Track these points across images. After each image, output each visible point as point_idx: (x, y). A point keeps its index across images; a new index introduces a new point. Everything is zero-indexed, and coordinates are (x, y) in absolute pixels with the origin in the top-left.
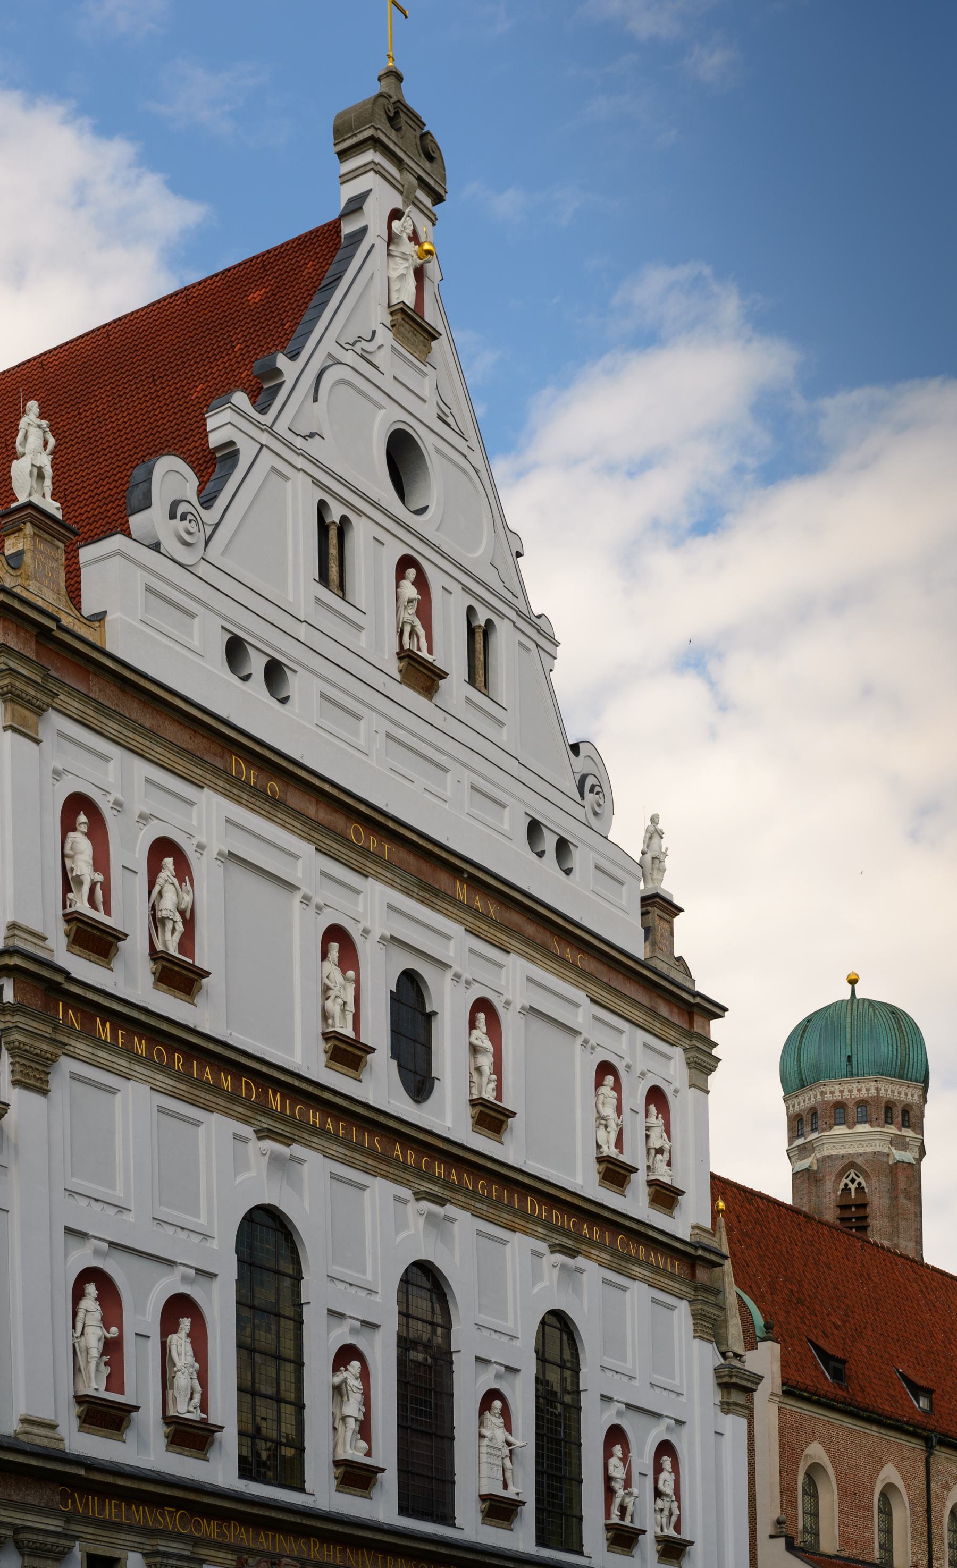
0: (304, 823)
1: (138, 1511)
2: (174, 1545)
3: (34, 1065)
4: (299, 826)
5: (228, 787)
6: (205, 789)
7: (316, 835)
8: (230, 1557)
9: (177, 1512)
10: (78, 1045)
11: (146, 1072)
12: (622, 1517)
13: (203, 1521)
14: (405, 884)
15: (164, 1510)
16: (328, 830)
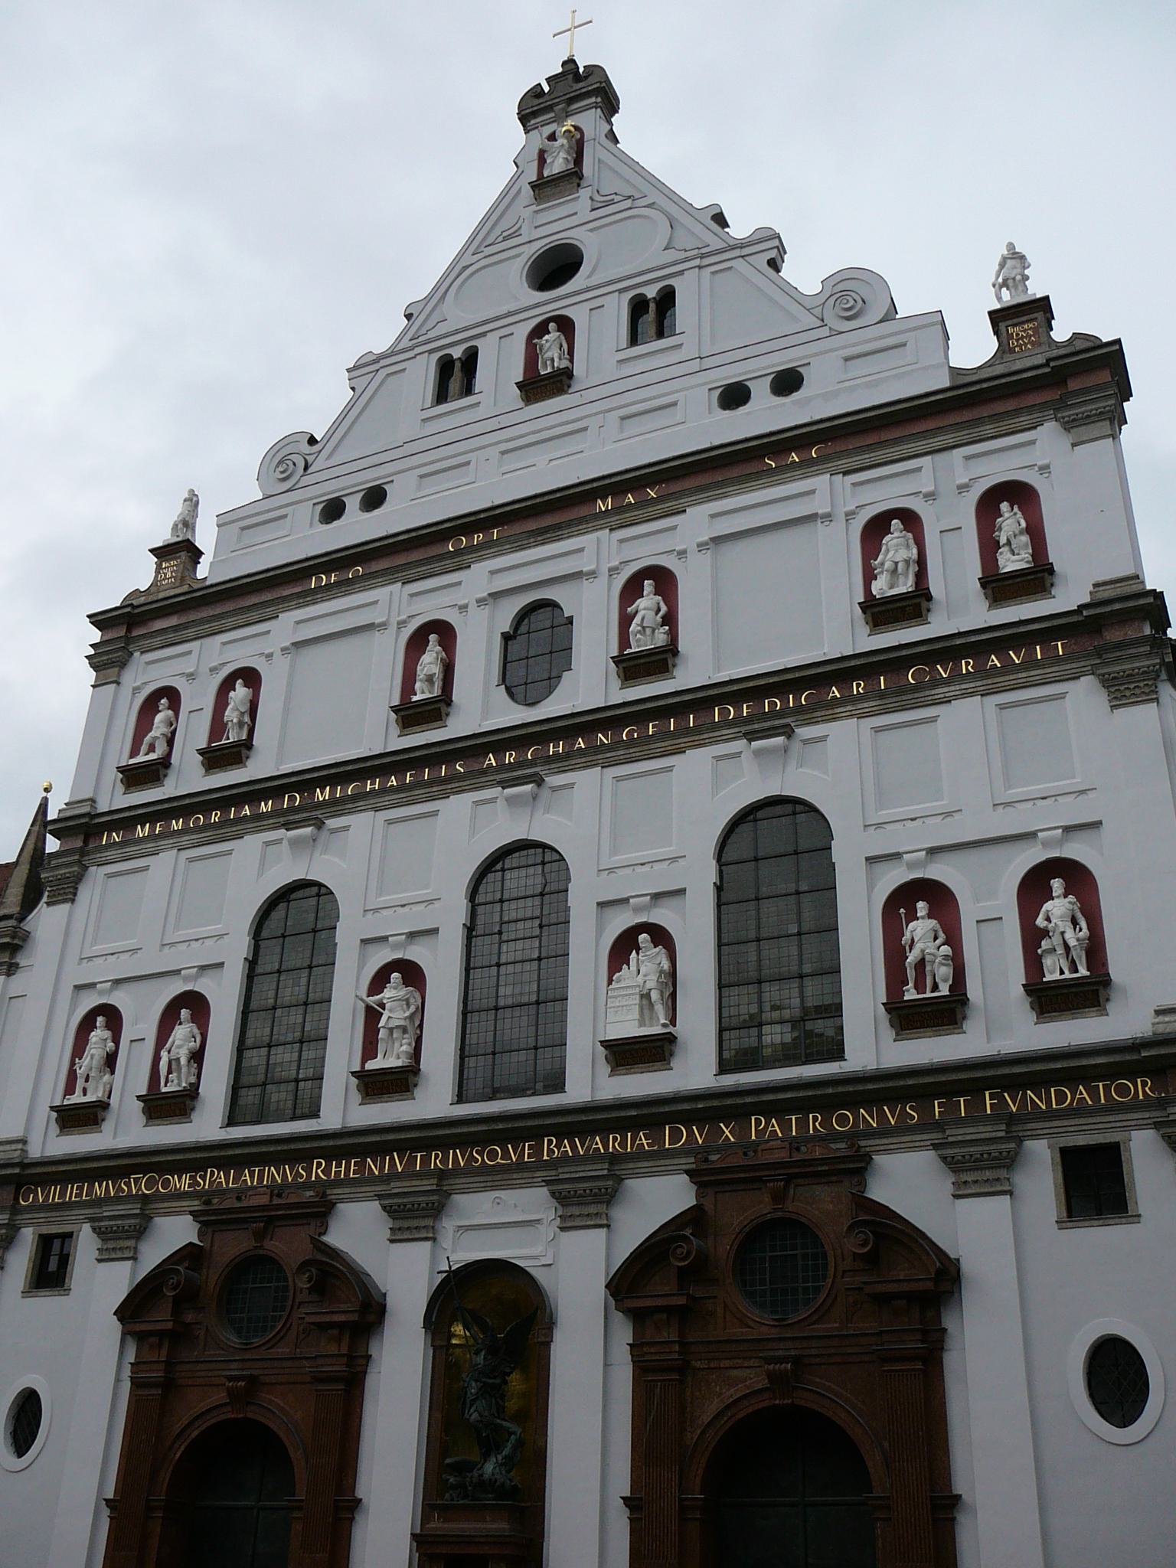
0: (383, 575)
1: (100, 1187)
2: (120, 1207)
3: (60, 887)
4: (380, 580)
5: (301, 601)
6: (280, 615)
7: (400, 575)
8: (196, 1203)
9: (143, 1177)
10: (109, 854)
11: (171, 841)
12: (920, 987)
13: (173, 1178)
14: (516, 545)
15: (130, 1178)
16: (397, 569)
